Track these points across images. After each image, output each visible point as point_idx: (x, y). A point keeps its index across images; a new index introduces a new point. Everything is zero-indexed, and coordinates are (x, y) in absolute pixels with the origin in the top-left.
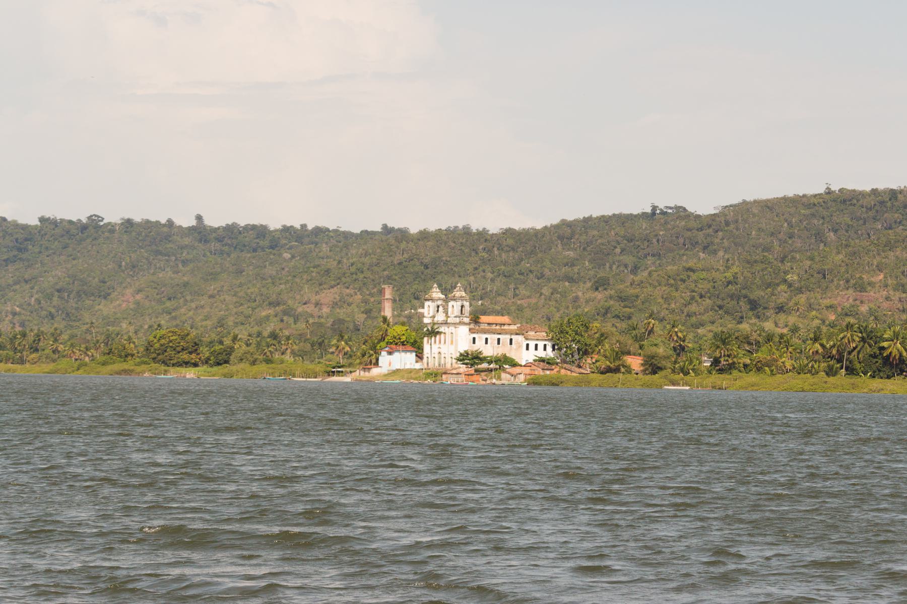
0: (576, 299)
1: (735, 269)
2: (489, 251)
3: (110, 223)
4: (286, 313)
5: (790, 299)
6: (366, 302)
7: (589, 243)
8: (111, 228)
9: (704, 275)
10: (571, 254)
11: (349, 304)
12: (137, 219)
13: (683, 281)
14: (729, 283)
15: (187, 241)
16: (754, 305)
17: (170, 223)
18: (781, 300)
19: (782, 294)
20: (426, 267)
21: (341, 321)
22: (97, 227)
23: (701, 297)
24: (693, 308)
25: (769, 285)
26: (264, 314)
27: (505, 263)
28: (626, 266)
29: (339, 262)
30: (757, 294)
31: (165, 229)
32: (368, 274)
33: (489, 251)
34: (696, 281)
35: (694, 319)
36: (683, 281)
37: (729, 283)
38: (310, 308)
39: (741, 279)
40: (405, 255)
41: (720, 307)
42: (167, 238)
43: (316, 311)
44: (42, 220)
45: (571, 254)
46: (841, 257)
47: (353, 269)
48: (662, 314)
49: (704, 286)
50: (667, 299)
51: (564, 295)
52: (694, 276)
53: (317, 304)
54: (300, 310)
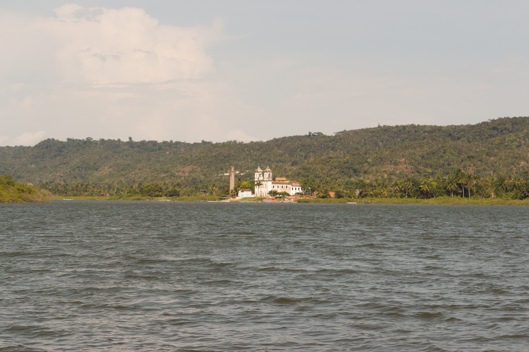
0: (286, 169)
1: (347, 157)
2: (249, 151)
3: (95, 141)
4: (171, 176)
5: (369, 168)
6: (202, 171)
7: (287, 148)
8: (96, 142)
9: (336, 160)
10: (281, 152)
11: (196, 172)
12: (106, 139)
13: (328, 162)
14: (345, 163)
15: (126, 147)
16: (355, 171)
17: (119, 140)
18: (366, 169)
19: (366, 167)
20: (225, 157)
21: (195, 179)
22: (90, 142)
23: (335, 168)
24: (332, 172)
25: (361, 163)
26: (162, 176)
27: (255, 156)
28: (302, 156)
29: (191, 156)
30: (356, 167)
31: (117, 143)
32: (203, 160)
33: (249, 151)
34: (333, 162)
35: (332, 177)
36: (328, 162)
37: (345, 163)
38: (180, 174)
39: (350, 161)
40: (217, 153)
41: (342, 172)
42: (118, 146)
43: (183, 175)
44: (68, 139)
45: (281, 152)
46: (388, 152)
47: (197, 158)
48: (320, 175)
49: (336, 164)
50: (322, 169)
51: (280, 168)
52: (332, 160)
53: (183, 172)
54: (177, 174)
